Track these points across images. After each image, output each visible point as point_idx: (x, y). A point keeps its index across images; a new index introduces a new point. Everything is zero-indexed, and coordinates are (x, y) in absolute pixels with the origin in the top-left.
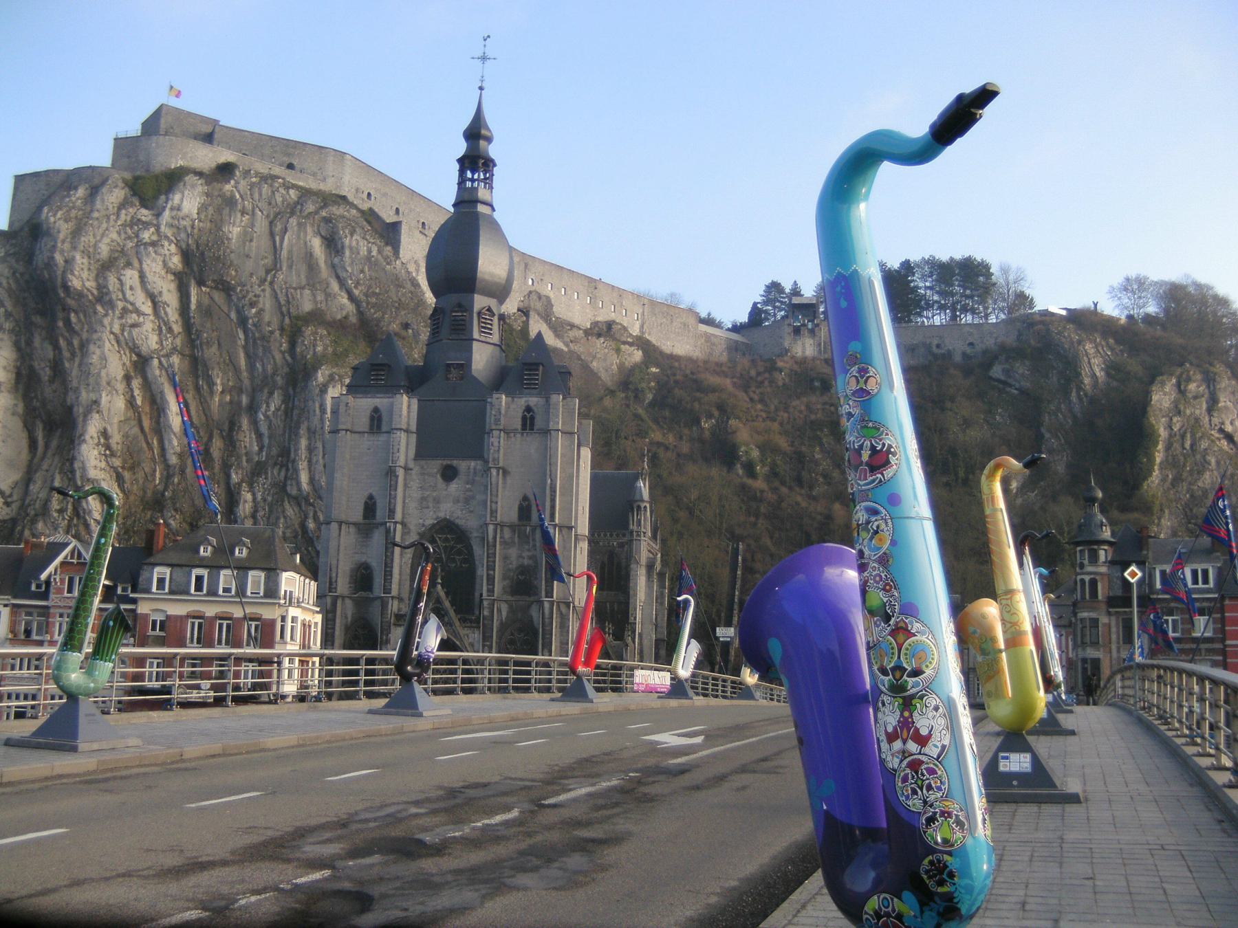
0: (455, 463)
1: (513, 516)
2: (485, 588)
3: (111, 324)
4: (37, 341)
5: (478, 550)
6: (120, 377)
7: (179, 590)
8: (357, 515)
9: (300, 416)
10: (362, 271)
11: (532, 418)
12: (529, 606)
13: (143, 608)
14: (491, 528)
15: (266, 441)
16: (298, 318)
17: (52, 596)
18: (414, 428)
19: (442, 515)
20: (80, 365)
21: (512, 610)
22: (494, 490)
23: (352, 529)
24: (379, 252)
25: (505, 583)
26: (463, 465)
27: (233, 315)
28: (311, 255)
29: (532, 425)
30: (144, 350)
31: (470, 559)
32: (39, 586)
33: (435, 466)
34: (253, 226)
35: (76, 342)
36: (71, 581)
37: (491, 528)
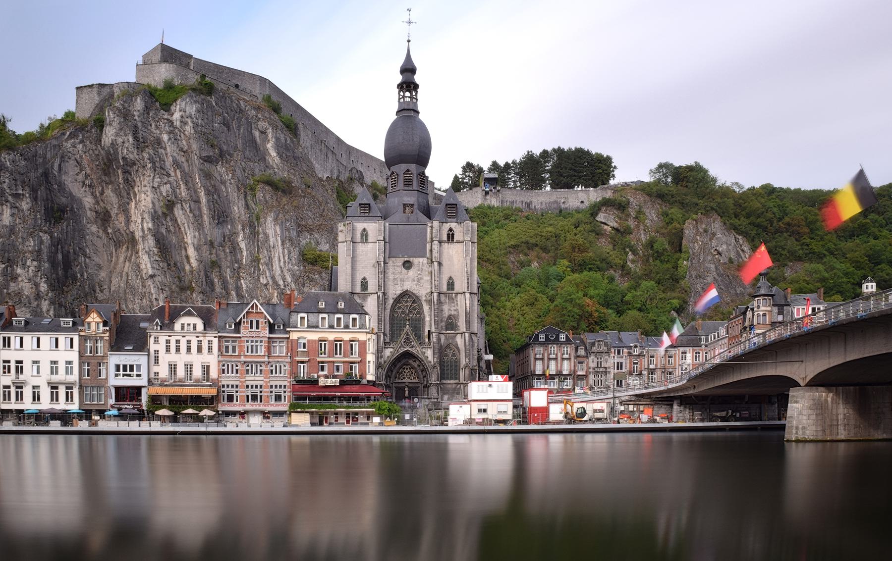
0: (411, 259)
1: (444, 288)
4: (109, 192)
5: (426, 308)
6: (160, 213)
7: (313, 327)
8: (358, 289)
11: (453, 235)
13: (294, 336)
14: (435, 294)
15: (245, 253)
17: (242, 331)
18: (387, 240)
19: (405, 288)
21: (446, 338)
25: (443, 324)
26: (416, 261)
29: (453, 238)
31: (420, 312)
32: (230, 326)
33: (400, 261)
36: (252, 322)
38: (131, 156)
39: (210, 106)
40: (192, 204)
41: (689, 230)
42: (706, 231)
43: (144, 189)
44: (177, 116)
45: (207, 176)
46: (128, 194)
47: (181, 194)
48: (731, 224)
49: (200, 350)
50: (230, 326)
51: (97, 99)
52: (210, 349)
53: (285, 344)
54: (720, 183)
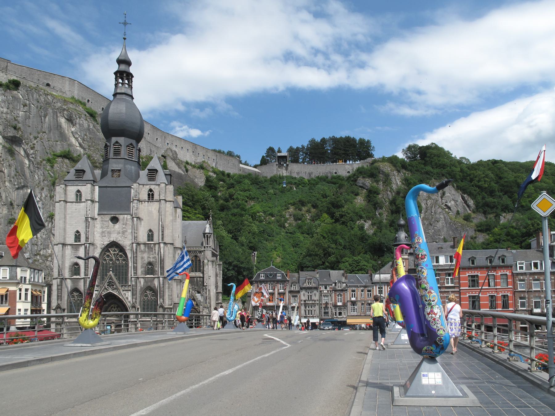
2: (132, 272)
5: (129, 255)
8: (71, 239)
10: (86, 135)
12: (153, 280)
19: (112, 240)
21: (145, 282)
22: (135, 227)
23: (69, 247)
24: (94, 126)
25: (143, 269)
28: (61, 127)
33: (108, 218)
34: (30, 112)
48: (457, 186)
54: (453, 156)
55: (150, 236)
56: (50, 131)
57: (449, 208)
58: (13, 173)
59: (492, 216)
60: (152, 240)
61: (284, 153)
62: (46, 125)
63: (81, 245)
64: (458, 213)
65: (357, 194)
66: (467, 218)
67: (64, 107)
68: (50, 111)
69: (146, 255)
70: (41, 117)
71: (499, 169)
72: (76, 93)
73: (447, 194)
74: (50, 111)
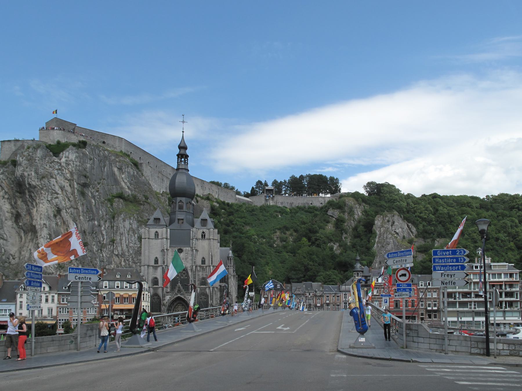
1: (199, 263)
3: (47, 197)
4: (19, 202)
5: (190, 273)
8: (152, 263)
9: (117, 229)
14: (194, 267)
16: (113, 196)
20: (37, 211)
23: (151, 267)
24: (137, 173)
27: (90, 194)
30: (61, 207)
31: (187, 275)
32: (65, 288)
35: (34, 204)
37: (194, 267)
38: (34, 183)
39: (84, 154)
40: (72, 209)
41: (378, 222)
42: (388, 221)
43: (41, 201)
44: (63, 160)
45: (83, 194)
46: (33, 204)
47: (65, 204)
48: (404, 217)
49: (47, 300)
50: (65, 288)
51: (14, 149)
52: (53, 300)
53: (96, 297)
55: (203, 262)
56: (108, 178)
57: (397, 234)
58: (85, 210)
59: (429, 240)
60: (205, 264)
61: (270, 187)
62: (105, 174)
63: (159, 266)
64: (404, 237)
65: (328, 222)
66: (411, 242)
67: (117, 160)
68: (107, 162)
69: (201, 273)
70: (101, 167)
71: (437, 202)
72: (124, 148)
73: (396, 223)
74: (107, 162)
